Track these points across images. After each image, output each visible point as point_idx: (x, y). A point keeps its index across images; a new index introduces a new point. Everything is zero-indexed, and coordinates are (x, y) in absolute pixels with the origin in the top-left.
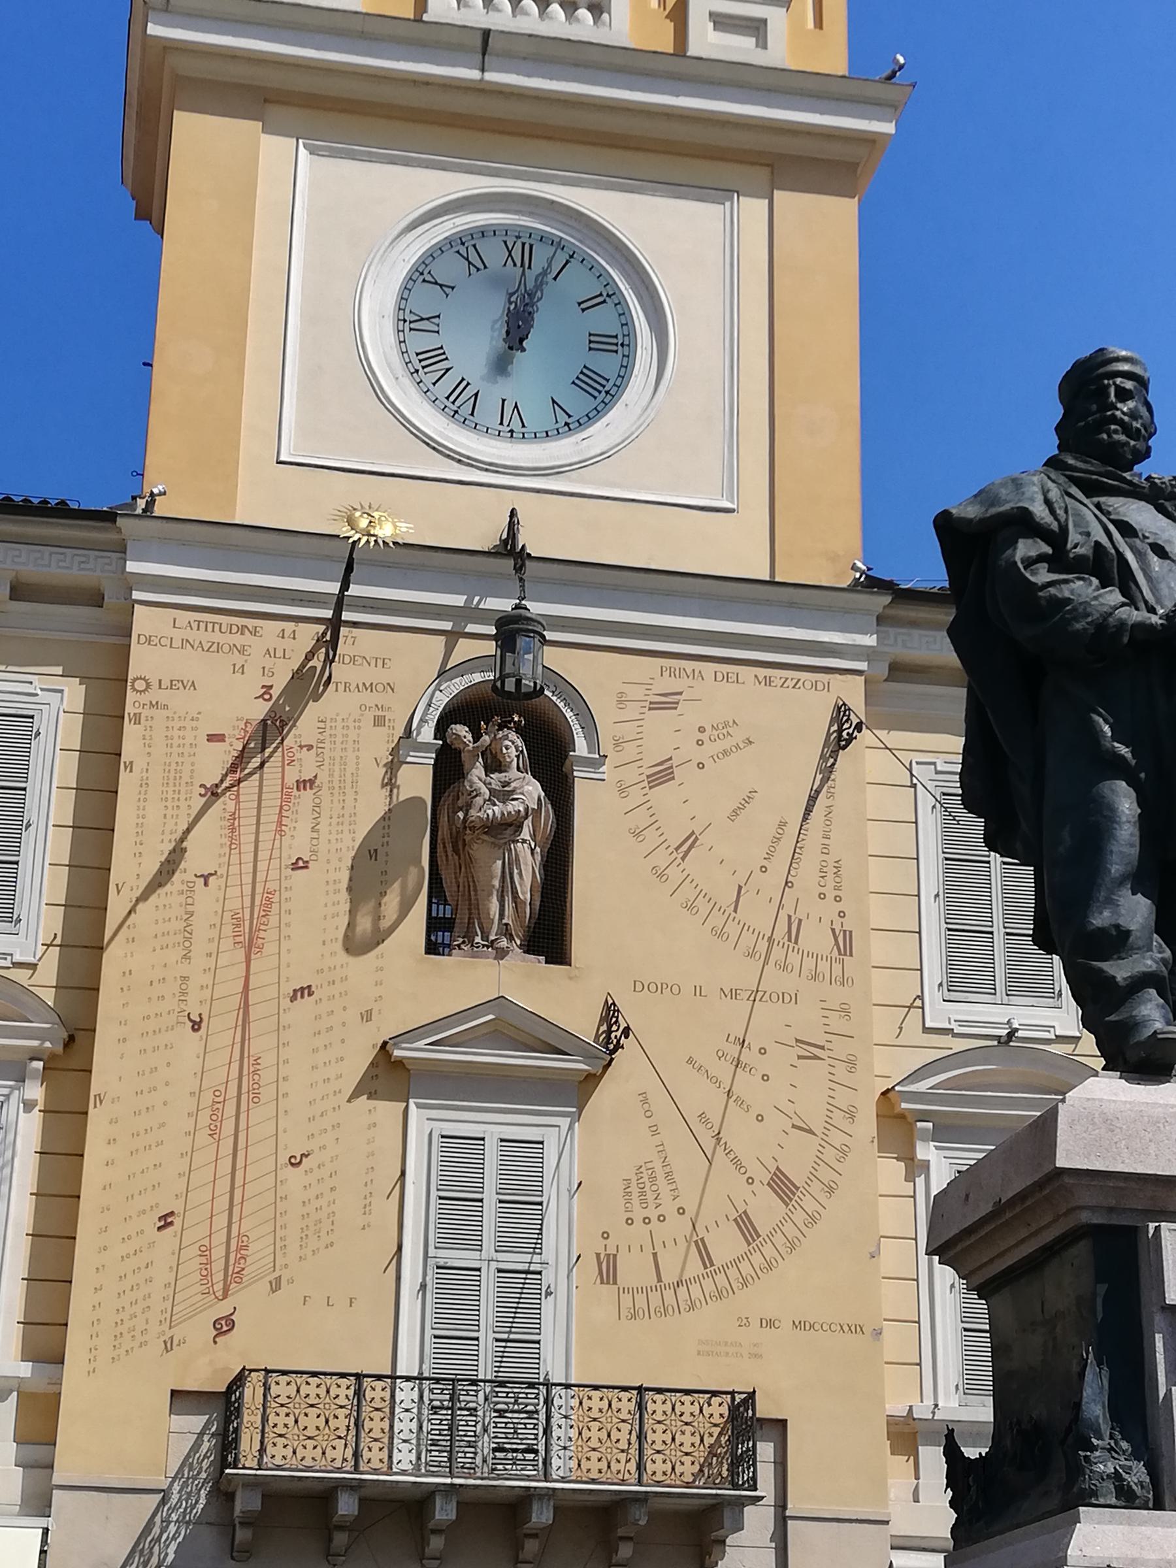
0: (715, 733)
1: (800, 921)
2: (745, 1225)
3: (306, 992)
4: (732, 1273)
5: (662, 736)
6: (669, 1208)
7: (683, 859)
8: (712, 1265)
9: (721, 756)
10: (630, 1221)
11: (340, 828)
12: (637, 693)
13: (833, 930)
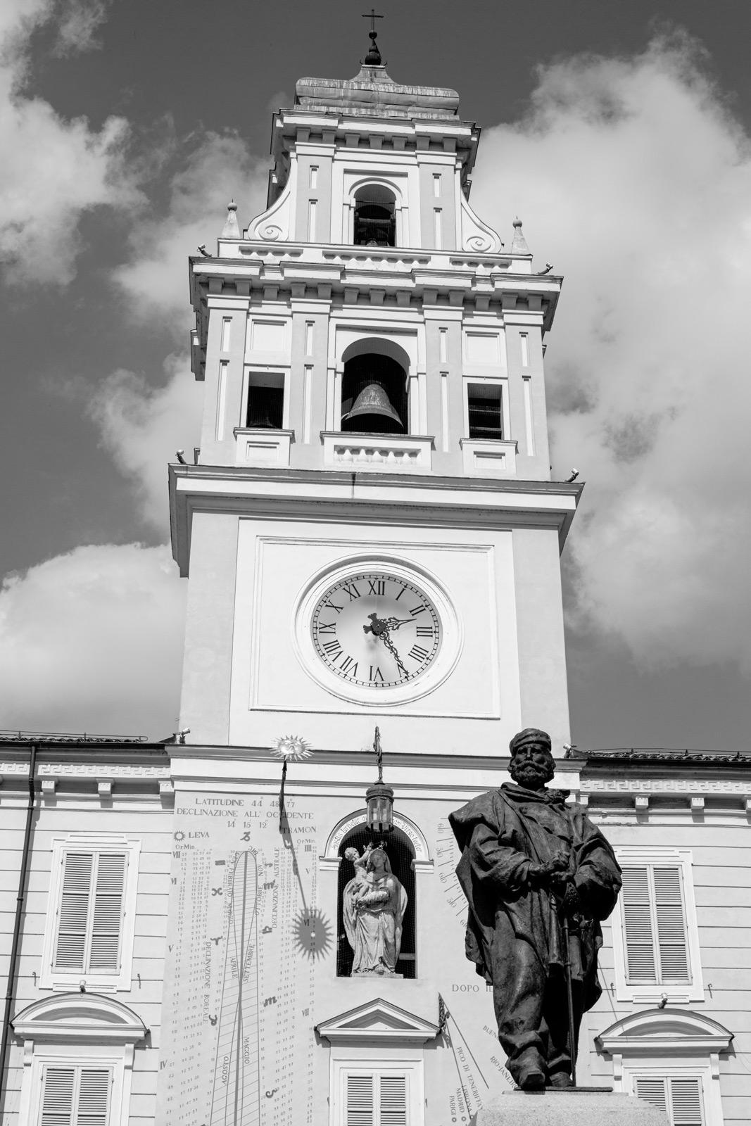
3: (272, 1001)
10: (454, 1120)
11: (288, 909)
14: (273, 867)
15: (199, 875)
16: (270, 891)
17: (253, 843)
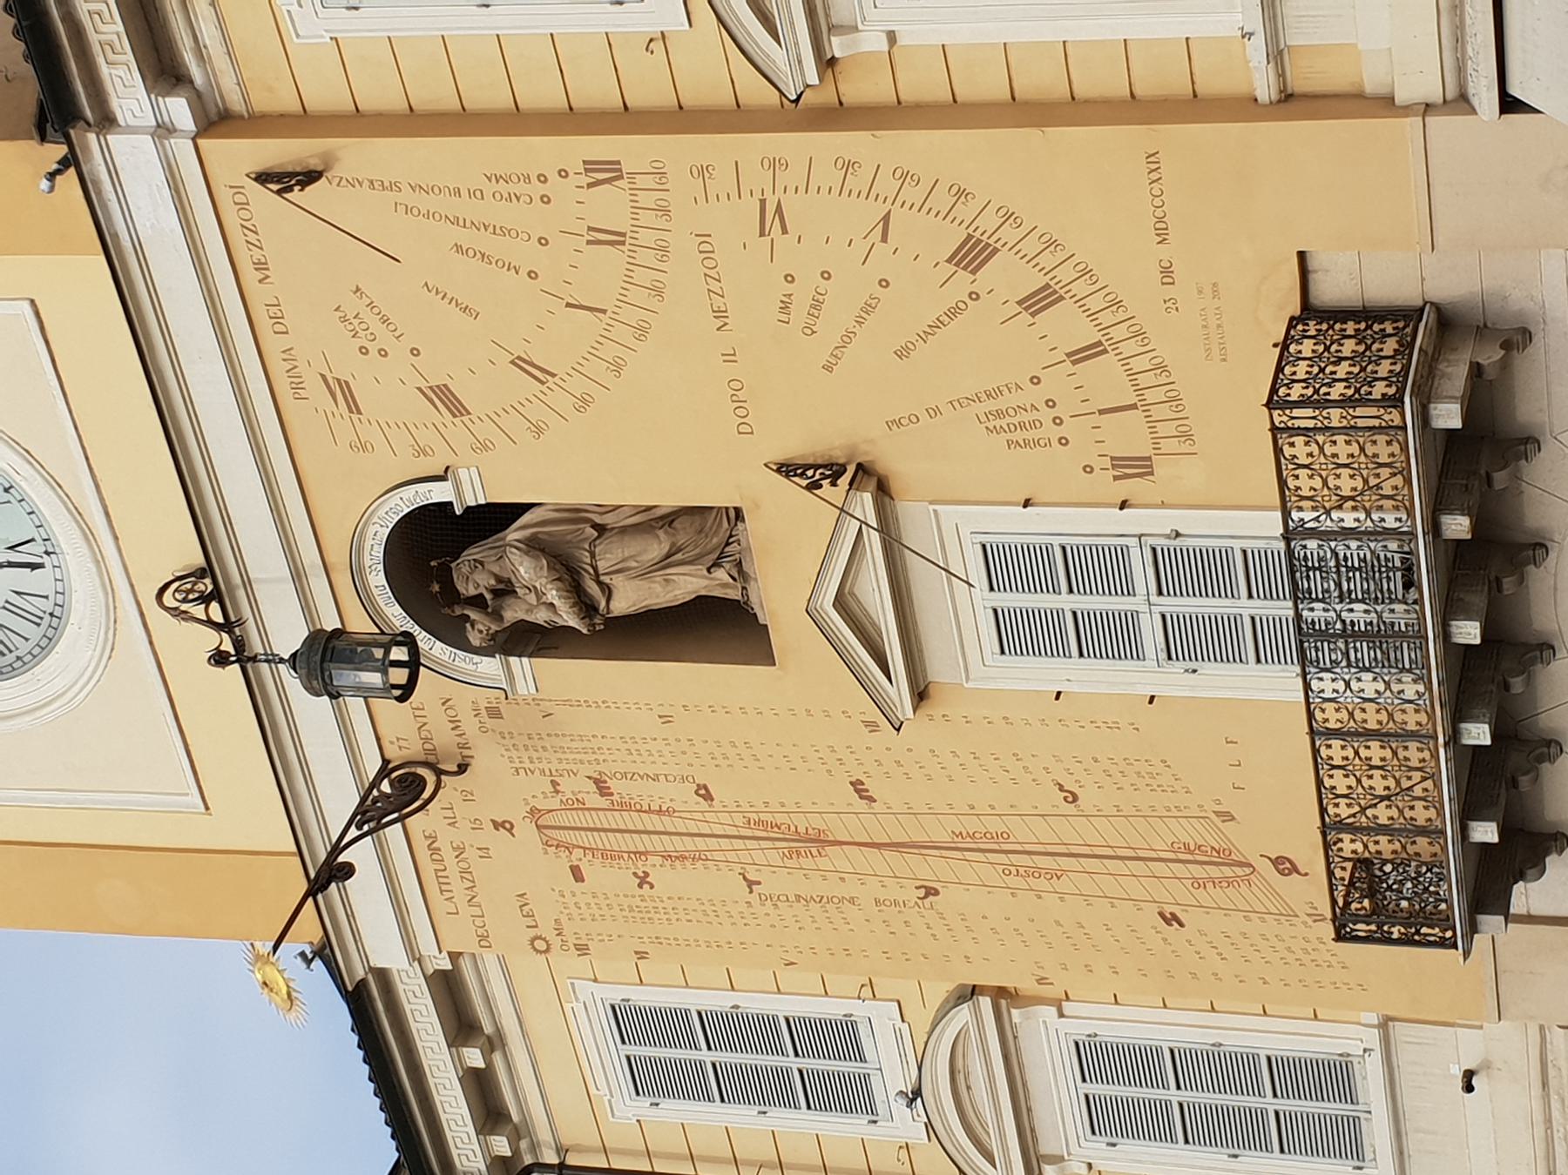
2: (1040, 301)
4: (1106, 318)
5: (389, 391)
6: (1036, 395)
7: (553, 375)
8: (1099, 343)
9: (392, 327)
10: (1064, 442)
17: (517, 815)
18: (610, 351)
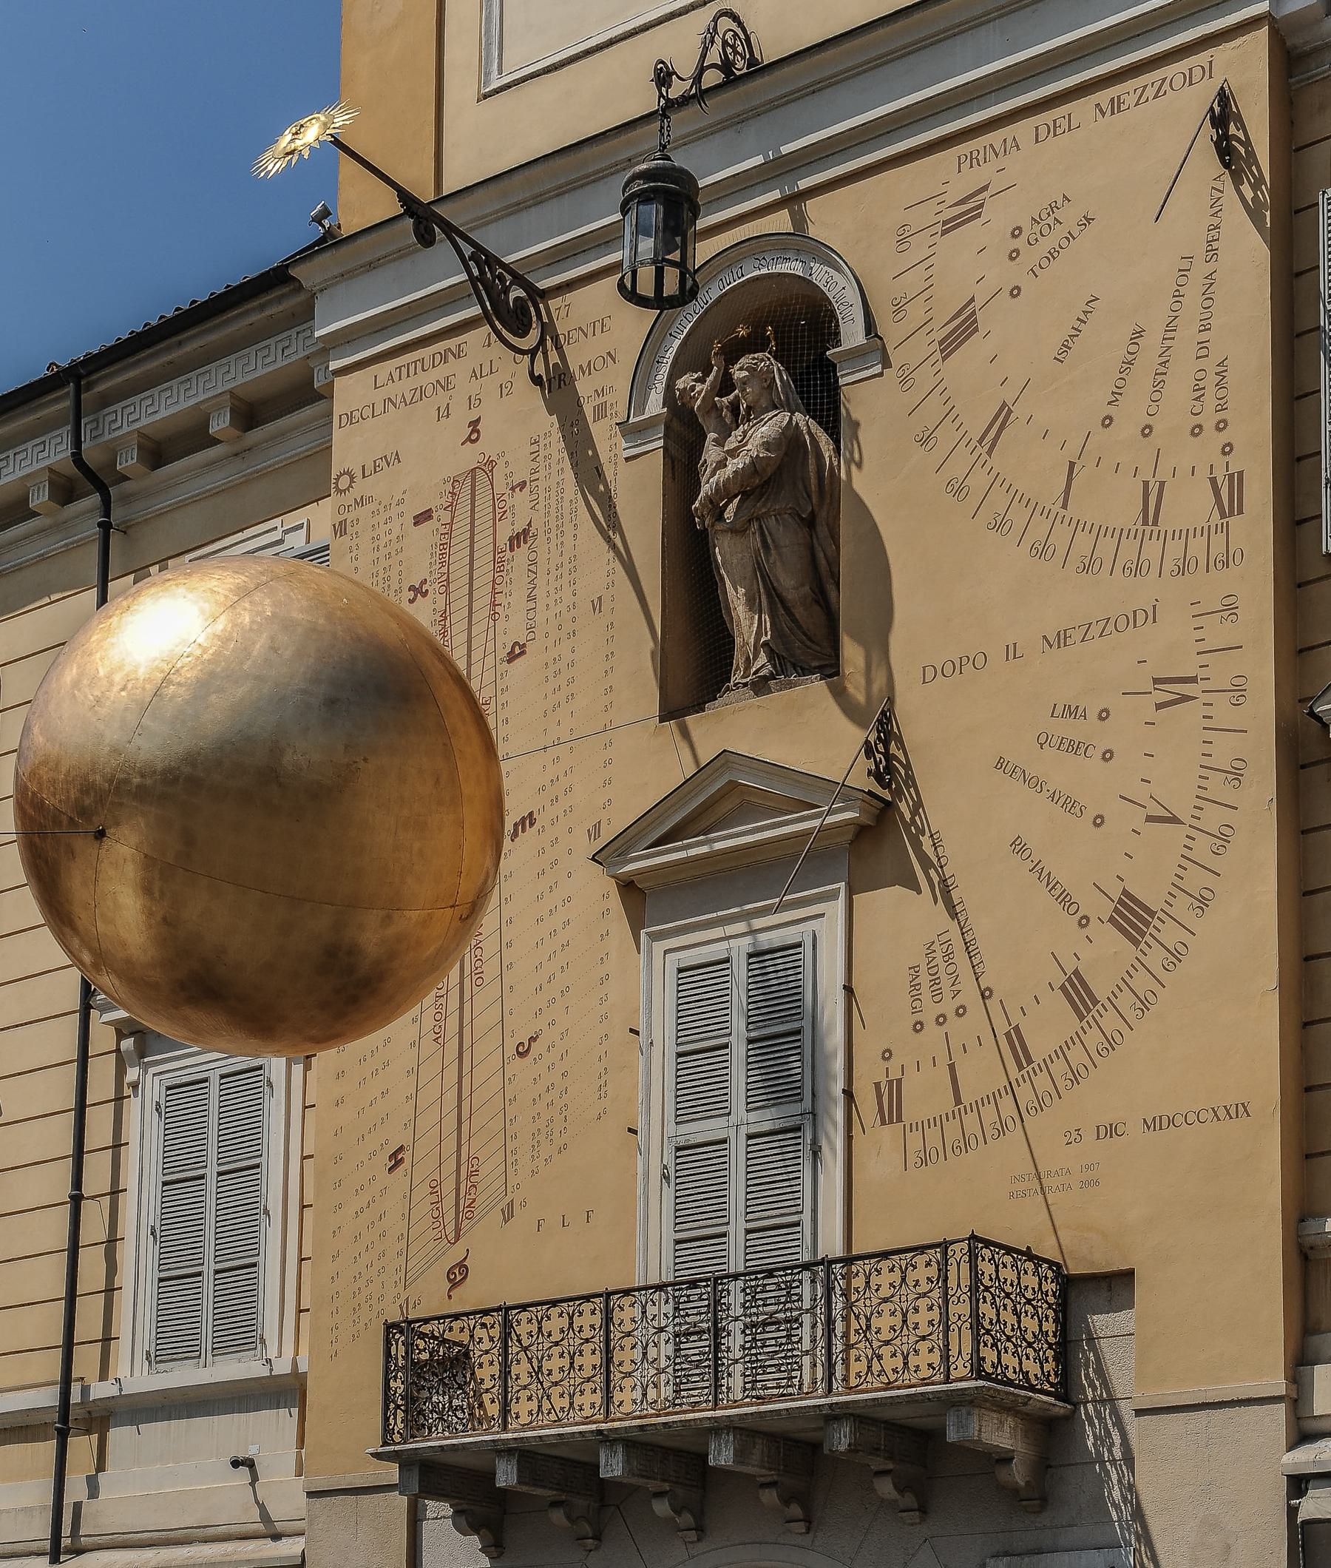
0: (1037, 228)
1: (1162, 484)
2: (1078, 993)
4: (1058, 1067)
6: (970, 995)
7: (990, 452)
8: (1030, 1061)
9: (1044, 263)
10: (918, 1027)
12: (928, 215)
13: (1213, 481)
14: (527, 489)
15: (383, 563)
16: (522, 552)
17: (487, 446)
18: (1018, 517)
